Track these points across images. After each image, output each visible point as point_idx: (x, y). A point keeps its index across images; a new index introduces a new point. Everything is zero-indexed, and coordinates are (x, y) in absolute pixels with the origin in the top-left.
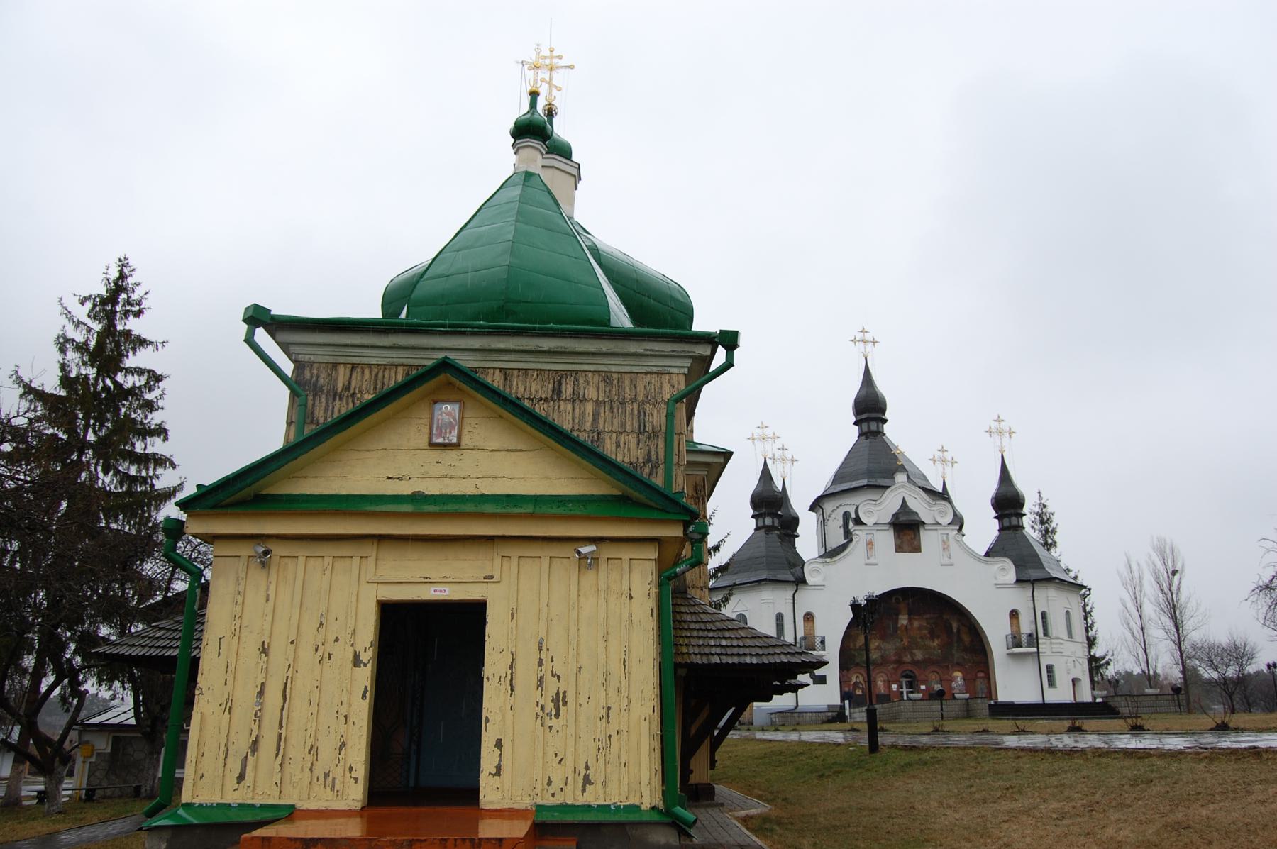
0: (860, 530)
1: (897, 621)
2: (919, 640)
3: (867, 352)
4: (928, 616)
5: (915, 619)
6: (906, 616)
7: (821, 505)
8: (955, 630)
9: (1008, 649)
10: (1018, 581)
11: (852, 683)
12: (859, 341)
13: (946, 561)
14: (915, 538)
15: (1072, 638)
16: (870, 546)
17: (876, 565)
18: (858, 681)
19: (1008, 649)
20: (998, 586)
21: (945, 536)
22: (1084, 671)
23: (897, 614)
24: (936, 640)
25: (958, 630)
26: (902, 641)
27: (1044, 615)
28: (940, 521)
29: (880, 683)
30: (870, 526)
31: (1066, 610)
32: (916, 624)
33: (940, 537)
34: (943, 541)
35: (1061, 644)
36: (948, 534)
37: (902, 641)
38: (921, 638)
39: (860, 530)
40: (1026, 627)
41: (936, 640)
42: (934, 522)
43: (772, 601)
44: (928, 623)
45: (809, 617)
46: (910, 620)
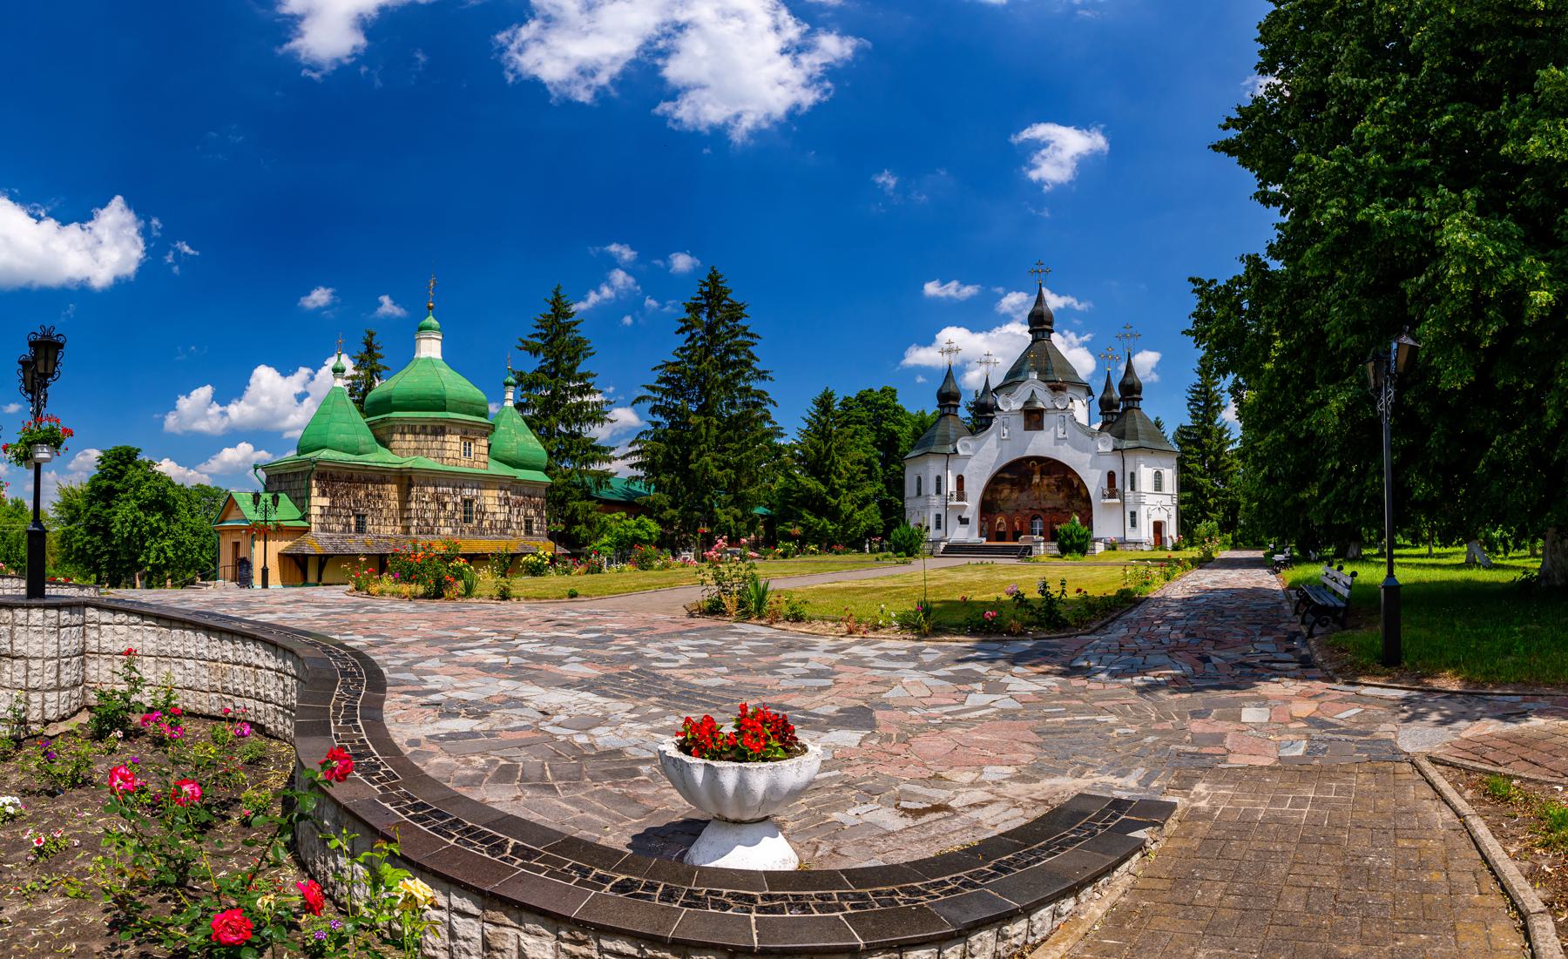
10: (1115, 450)
22: (1169, 516)
27: (1133, 475)
32: (1045, 482)
40: (1118, 485)
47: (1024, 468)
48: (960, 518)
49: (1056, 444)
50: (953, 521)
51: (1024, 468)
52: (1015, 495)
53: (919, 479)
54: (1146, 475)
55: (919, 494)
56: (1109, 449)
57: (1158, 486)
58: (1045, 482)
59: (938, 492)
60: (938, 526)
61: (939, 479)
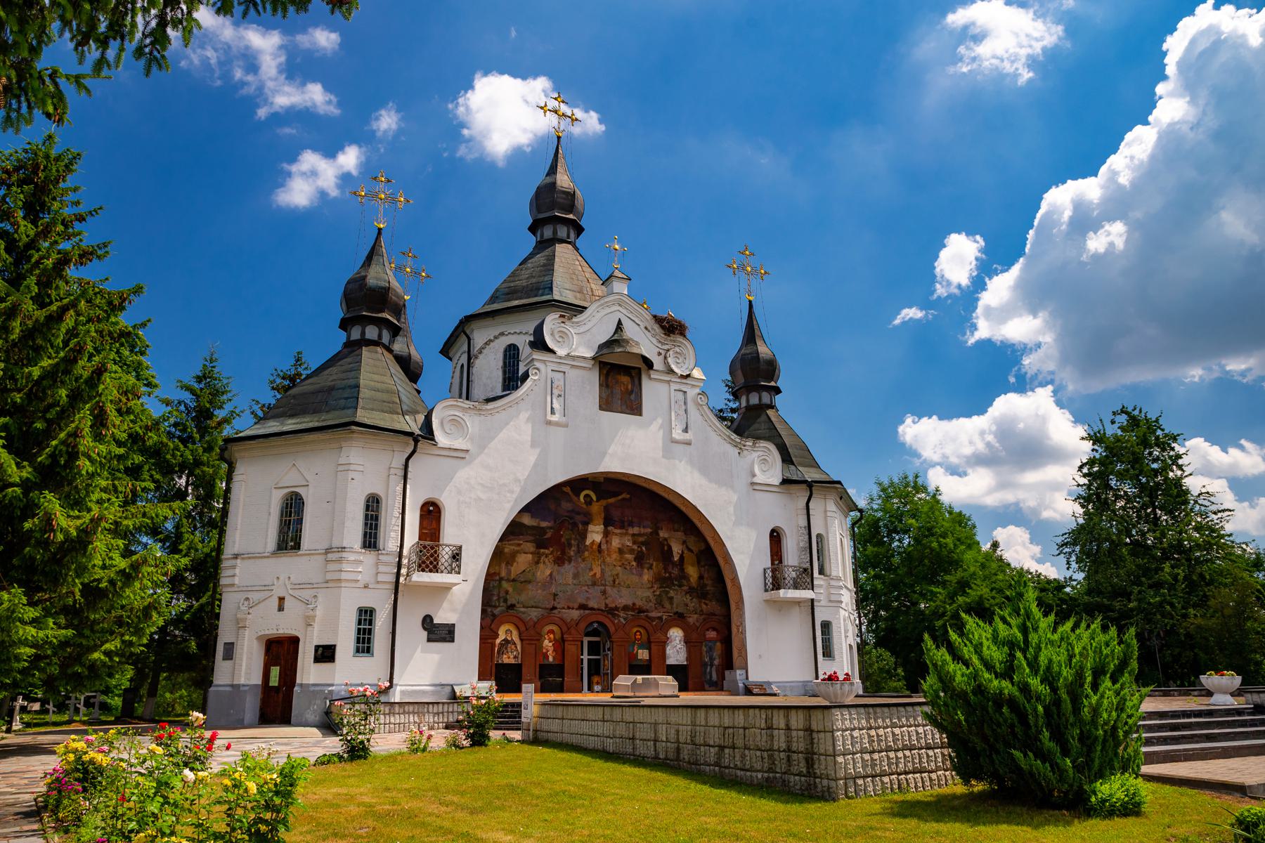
0: (544, 362)
1: (583, 536)
3: (561, 129)
4: (636, 530)
5: (616, 535)
6: (600, 528)
7: (468, 332)
9: (766, 590)
10: (786, 482)
11: (498, 641)
12: (550, 111)
13: (678, 434)
18: (510, 639)
19: (766, 590)
23: (586, 524)
25: (682, 557)
28: (673, 367)
29: (547, 644)
30: (560, 358)
32: (616, 542)
36: (685, 392)
39: (544, 362)
43: (361, 468)
44: (634, 543)
46: (606, 534)
47: (566, 506)
48: (427, 622)
49: (667, 453)
50: (410, 629)
51: (566, 506)
52: (545, 571)
53: (293, 508)
56: (776, 480)
58: (616, 542)
59: (371, 541)
60: (364, 644)
61: (373, 506)
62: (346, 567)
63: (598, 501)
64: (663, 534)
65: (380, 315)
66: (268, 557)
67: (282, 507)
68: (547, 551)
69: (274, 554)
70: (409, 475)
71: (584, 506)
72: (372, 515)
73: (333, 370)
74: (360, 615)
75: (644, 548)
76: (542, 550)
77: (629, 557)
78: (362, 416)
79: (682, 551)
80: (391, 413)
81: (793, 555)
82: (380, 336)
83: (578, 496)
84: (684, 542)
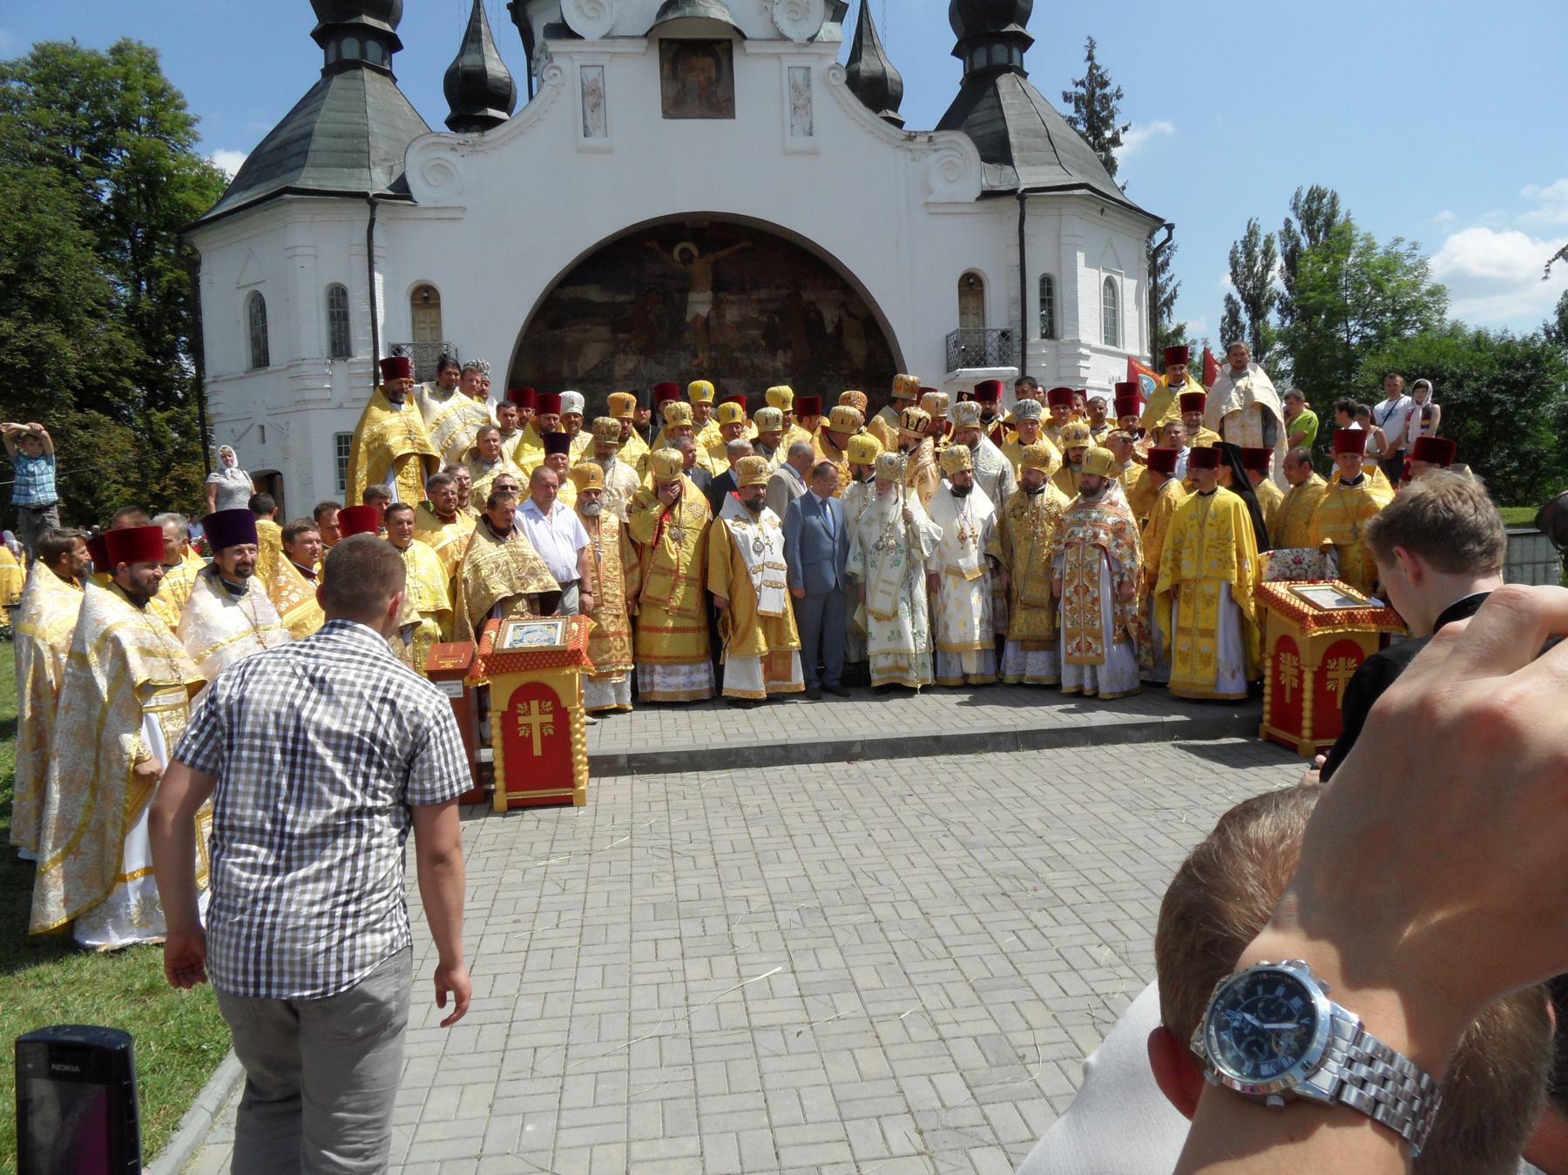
1: (682, 307)
2: (738, 354)
4: (763, 294)
5: (732, 303)
6: (707, 296)
8: (829, 330)
14: (718, 80)
15: (1114, 343)
16: (591, 100)
17: (609, 151)
20: (933, 210)
21: (799, 75)
23: (685, 291)
24: (781, 352)
25: (839, 327)
26: (696, 356)
27: (1047, 284)
28: (788, 29)
30: (593, 44)
31: (1104, 275)
32: (732, 314)
33: (785, 74)
34: (795, 87)
35: (1087, 358)
37: (696, 356)
38: (745, 348)
41: (781, 352)
42: (771, 34)
44: (762, 312)
45: (425, 298)
46: (717, 304)
53: (258, 309)
54: (1087, 285)
55: (261, 359)
57: (1112, 332)
58: (732, 314)
59: (340, 347)
61: (338, 298)
62: (308, 383)
63: (701, 256)
64: (807, 296)
65: (354, 21)
66: (242, 378)
67: (254, 311)
68: (626, 336)
69: (251, 370)
70: (376, 252)
71: (681, 266)
72: (339, 313)
73: (302, 113)
74: (339, 443)
75: (777, 320)
76: (621, 336)
77: (755, 333)
78: (308, 179)
79: (840, 320)
80: (353, 167)
81: (998, 312)
82: (363, 52)
83: (670, 252)
84: (843, 305)
